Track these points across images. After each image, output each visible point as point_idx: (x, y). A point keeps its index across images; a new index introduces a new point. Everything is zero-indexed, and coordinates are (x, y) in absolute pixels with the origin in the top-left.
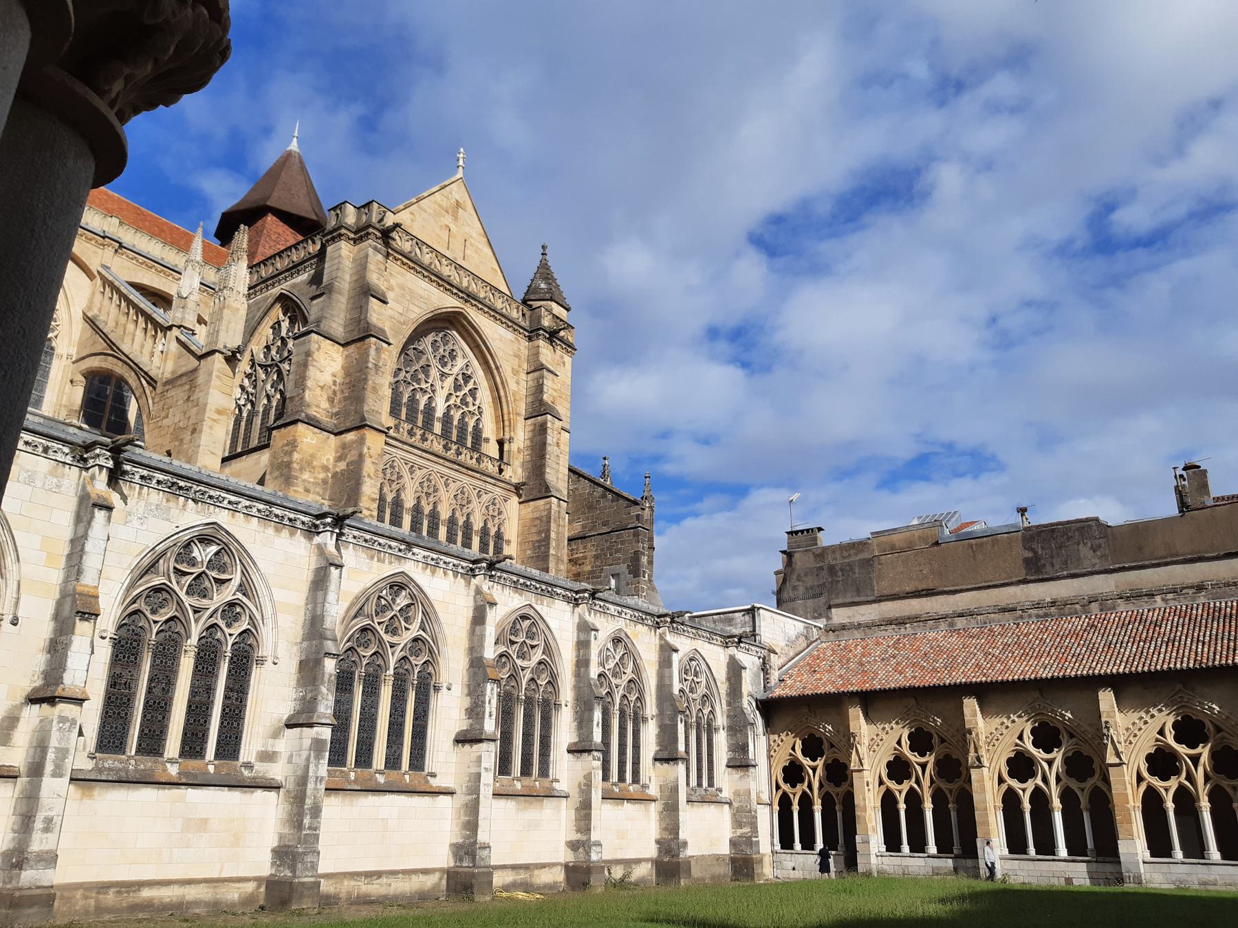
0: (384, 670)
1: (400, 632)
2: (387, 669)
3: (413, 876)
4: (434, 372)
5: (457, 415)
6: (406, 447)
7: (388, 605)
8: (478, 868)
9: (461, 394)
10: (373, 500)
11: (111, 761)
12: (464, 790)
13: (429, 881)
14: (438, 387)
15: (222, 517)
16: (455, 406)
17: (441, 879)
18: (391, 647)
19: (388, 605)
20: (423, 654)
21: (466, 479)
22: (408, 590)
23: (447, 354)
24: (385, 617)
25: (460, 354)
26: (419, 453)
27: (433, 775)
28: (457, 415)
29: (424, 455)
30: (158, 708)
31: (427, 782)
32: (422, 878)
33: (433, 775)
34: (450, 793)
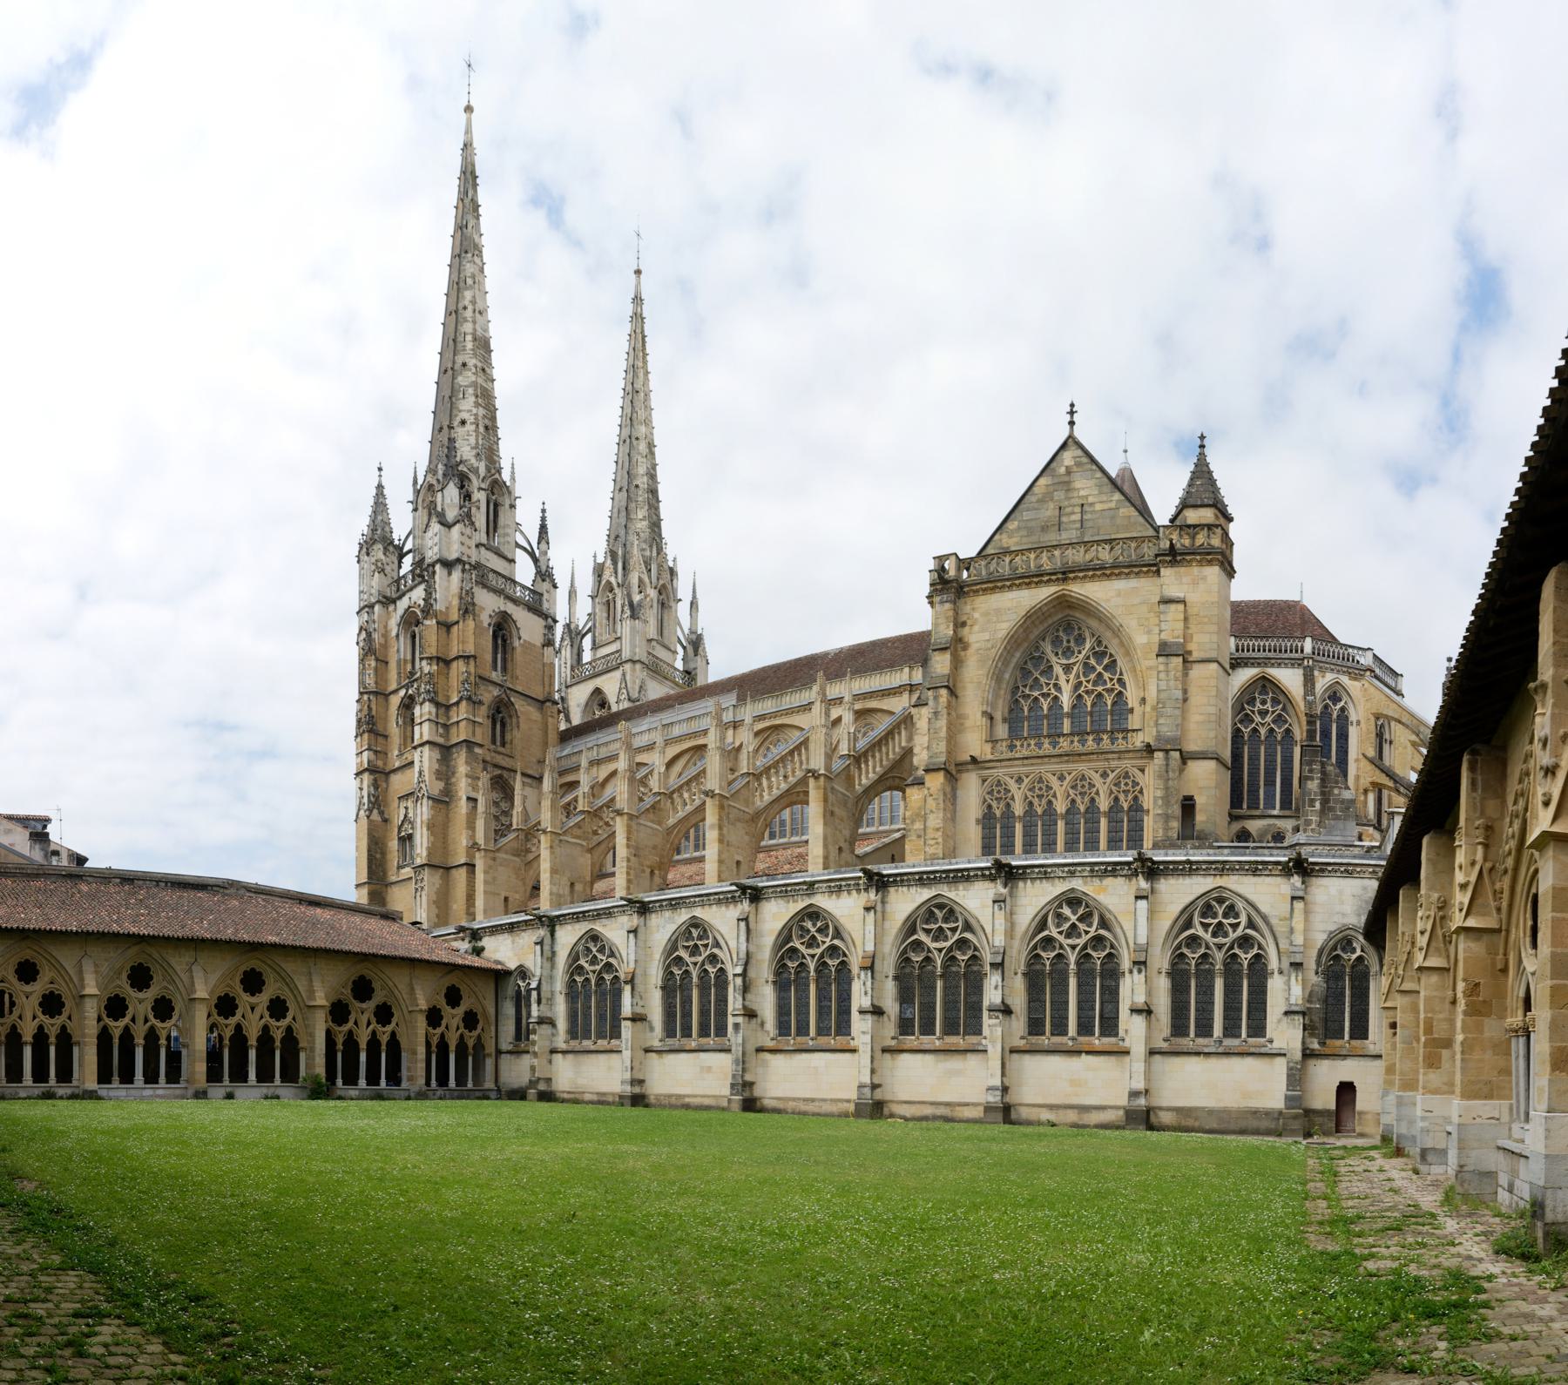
4: (1058, 670)
5: (1089, 701)
6: (1004, 764)
9: (1092, 676)
10: (938, 830)
11: (670, 1041)
14: (1062, 682)
15: (698, 912)
16: (1087, 692)
21: (1081, 767)
23: (1072, 644)
25: (1087, 635)
26: (1019, 762)
28: (1089, 701)
29: (1026, 762)
30: (687, 1015)
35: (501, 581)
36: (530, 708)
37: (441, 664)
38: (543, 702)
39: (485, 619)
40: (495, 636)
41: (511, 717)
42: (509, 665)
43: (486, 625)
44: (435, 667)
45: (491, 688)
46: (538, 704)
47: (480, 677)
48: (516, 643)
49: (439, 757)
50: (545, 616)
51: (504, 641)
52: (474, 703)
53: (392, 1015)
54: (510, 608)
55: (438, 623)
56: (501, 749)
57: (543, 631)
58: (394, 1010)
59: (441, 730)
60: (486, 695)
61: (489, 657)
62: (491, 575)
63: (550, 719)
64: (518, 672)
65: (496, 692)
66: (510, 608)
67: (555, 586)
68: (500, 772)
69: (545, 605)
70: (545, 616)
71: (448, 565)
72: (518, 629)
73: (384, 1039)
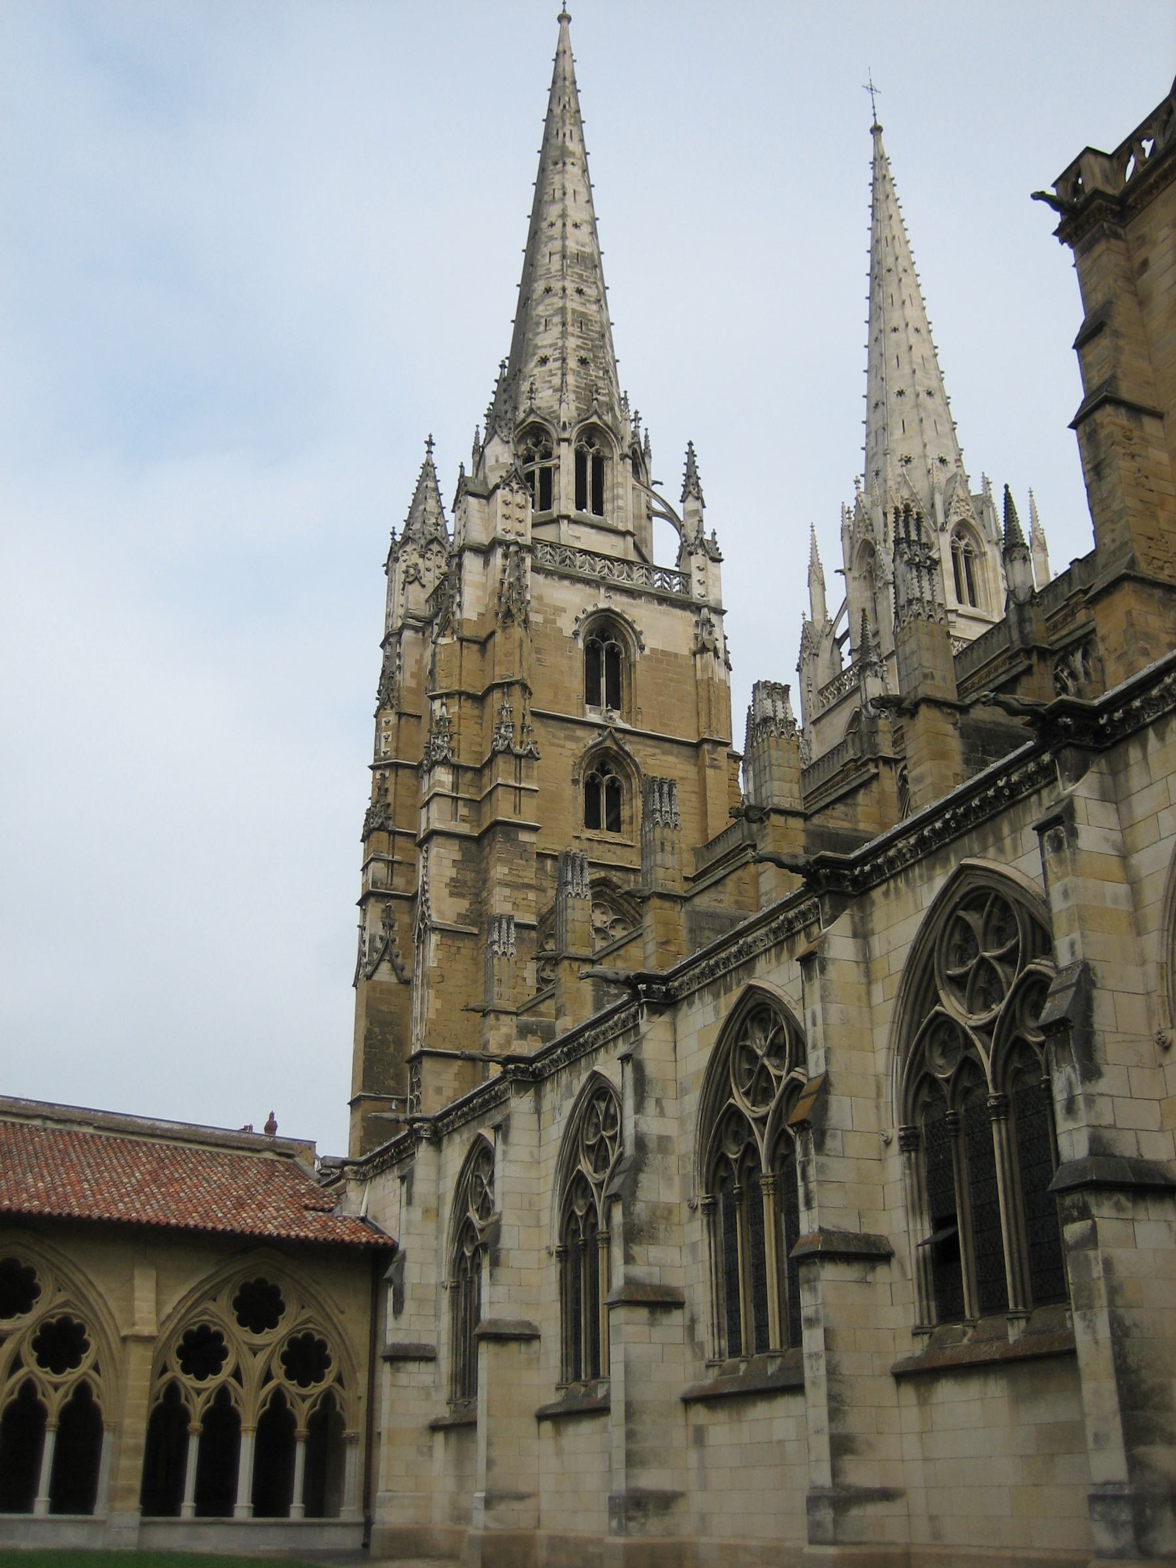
35: (600, 564)
36: (671, 759)
37: (468, 706)
38: (697, 746)
39: (567, 626)
40: (592, 650)
41: (628, 777)
42: (624, 694)
43: (568, 632)
44: (455, 709)
45: (580, 732)
46: (685, 751)
47: (534, 714)
48: (637, 656)
49: (457, 856)
50: (696, 608)
51: (613, 655)
52: (519, 757)
53: (85, 1346)
54: (618, 603)
55: (461, 640)
56: (611, 837)
57: (692, 631)
58: (89, 1336)
59: (463, 811)
60: (571, 745)
61: (577, 684)
62: (579, 559)
63: (710, 772)
64: (640, 702)
65: (591, 738)
66: (618, 603)
67: (717, 560)
68: (603, 874)
69: (696, 591)
70: (696, 608)
71: (484, 552)
72: (638, 634)
73: (54, 1402)
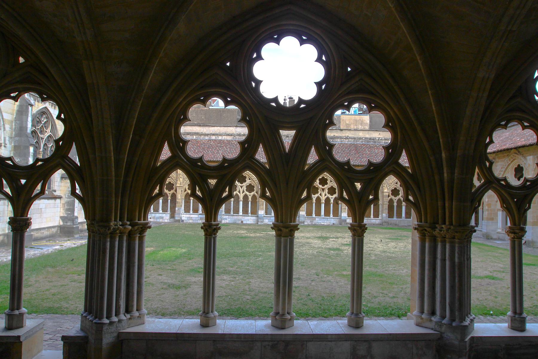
0: (38, 149)
1: (43, 133)
2: (40, 148)
3: (50, 229)
7: (39, 121)
8: (75, 225)
12: (67, 196)
13: (54, 230)
17: (58, 229)
18: (41, 139)
19: (39, 121)
20: (50, 142)
22: (46, 115)
24: (39, 126)
27: (55, 191)
31: (53, 194)
32: (53, 230)
33: (55, 191)
34: (60, 198)
